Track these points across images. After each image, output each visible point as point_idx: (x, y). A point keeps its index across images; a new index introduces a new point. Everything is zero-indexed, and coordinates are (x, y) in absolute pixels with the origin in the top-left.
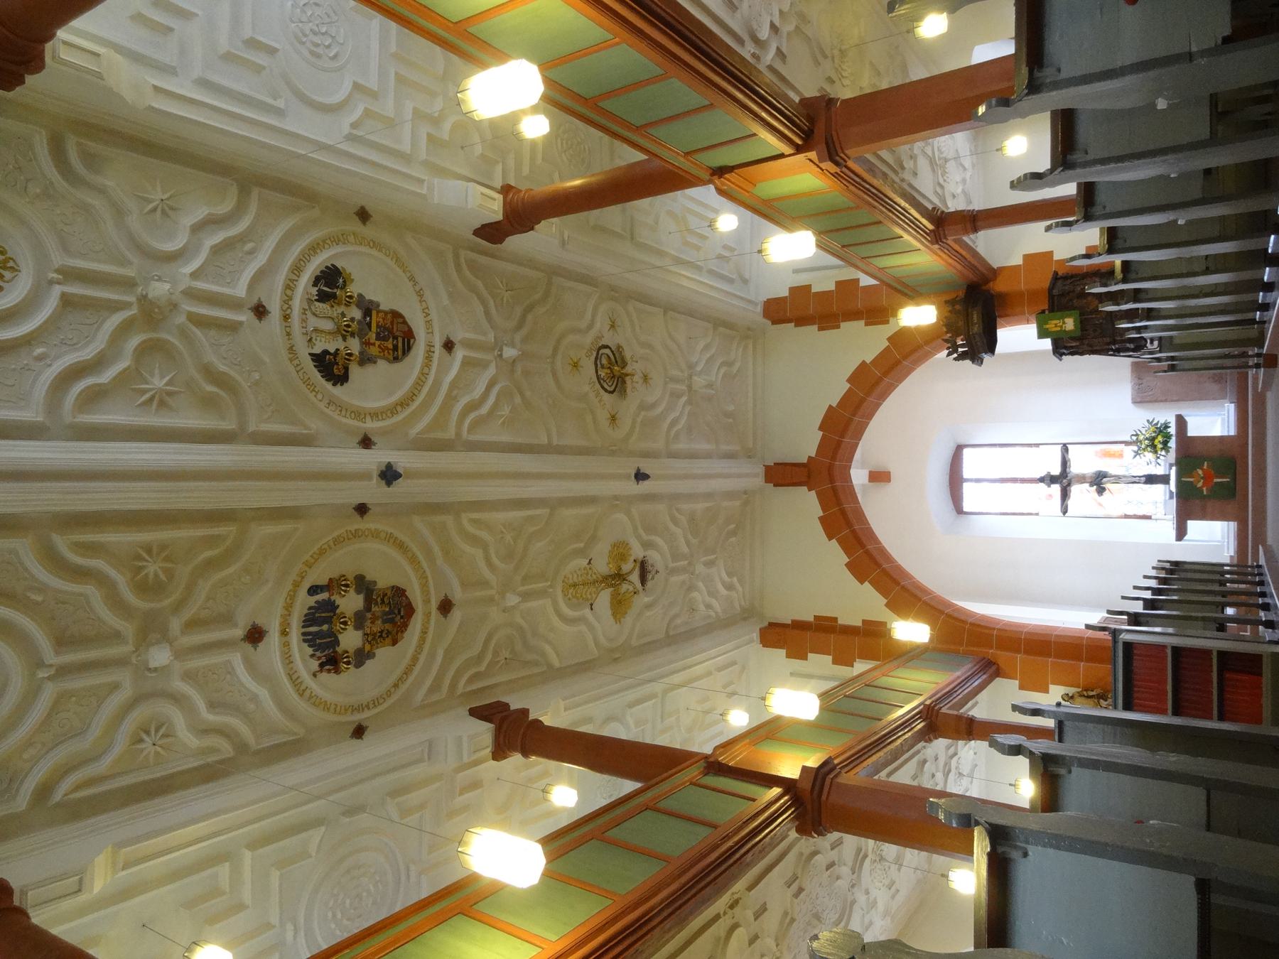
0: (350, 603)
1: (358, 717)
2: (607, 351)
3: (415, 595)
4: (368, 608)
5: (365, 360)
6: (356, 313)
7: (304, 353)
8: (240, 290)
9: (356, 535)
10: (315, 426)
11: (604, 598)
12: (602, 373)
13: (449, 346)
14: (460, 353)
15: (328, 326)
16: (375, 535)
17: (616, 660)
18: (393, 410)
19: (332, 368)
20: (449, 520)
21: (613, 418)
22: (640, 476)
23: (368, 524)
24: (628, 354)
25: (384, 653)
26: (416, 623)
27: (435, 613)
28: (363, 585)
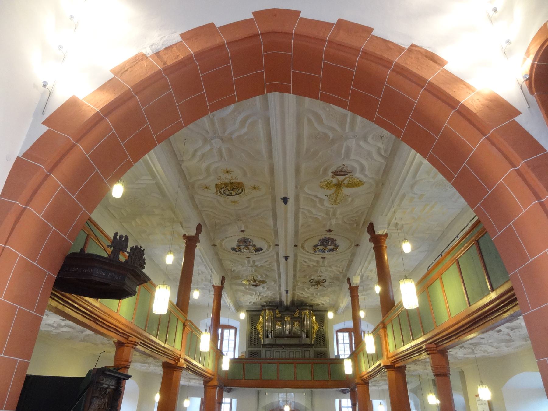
0: (321, 247)
1: (353, 245)
2: (222, 191)
3: (322, 237)
4: (324, 245)
5: (254, 246)
6: (242, 247)
7: (255, 253)
8: (246, 262)
9: (302, 246)
10: (274, 253)
11: (346, 191)
12: (234, 193)
13: (242, 231)
14: (243, 229)
15: (248, 251)
16: (303, 244)
17: (383, 184)
18: (267, 241)
19: (258, 250)
20: (300, 232)
21: (255, 188)
22: (285, 200)
23: (300, 245)
24: (218, 182)
25: (337, 242)
26: (331, 237)
27: (330, 233)
28: (316, 246)
